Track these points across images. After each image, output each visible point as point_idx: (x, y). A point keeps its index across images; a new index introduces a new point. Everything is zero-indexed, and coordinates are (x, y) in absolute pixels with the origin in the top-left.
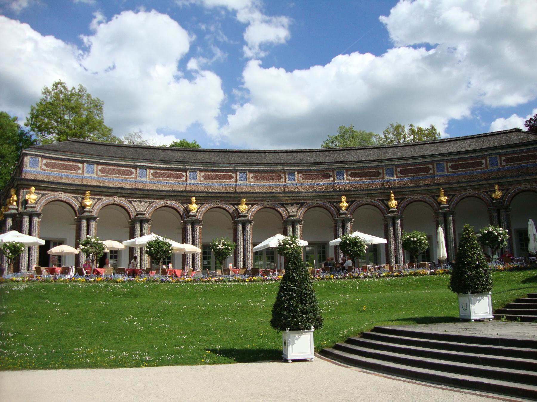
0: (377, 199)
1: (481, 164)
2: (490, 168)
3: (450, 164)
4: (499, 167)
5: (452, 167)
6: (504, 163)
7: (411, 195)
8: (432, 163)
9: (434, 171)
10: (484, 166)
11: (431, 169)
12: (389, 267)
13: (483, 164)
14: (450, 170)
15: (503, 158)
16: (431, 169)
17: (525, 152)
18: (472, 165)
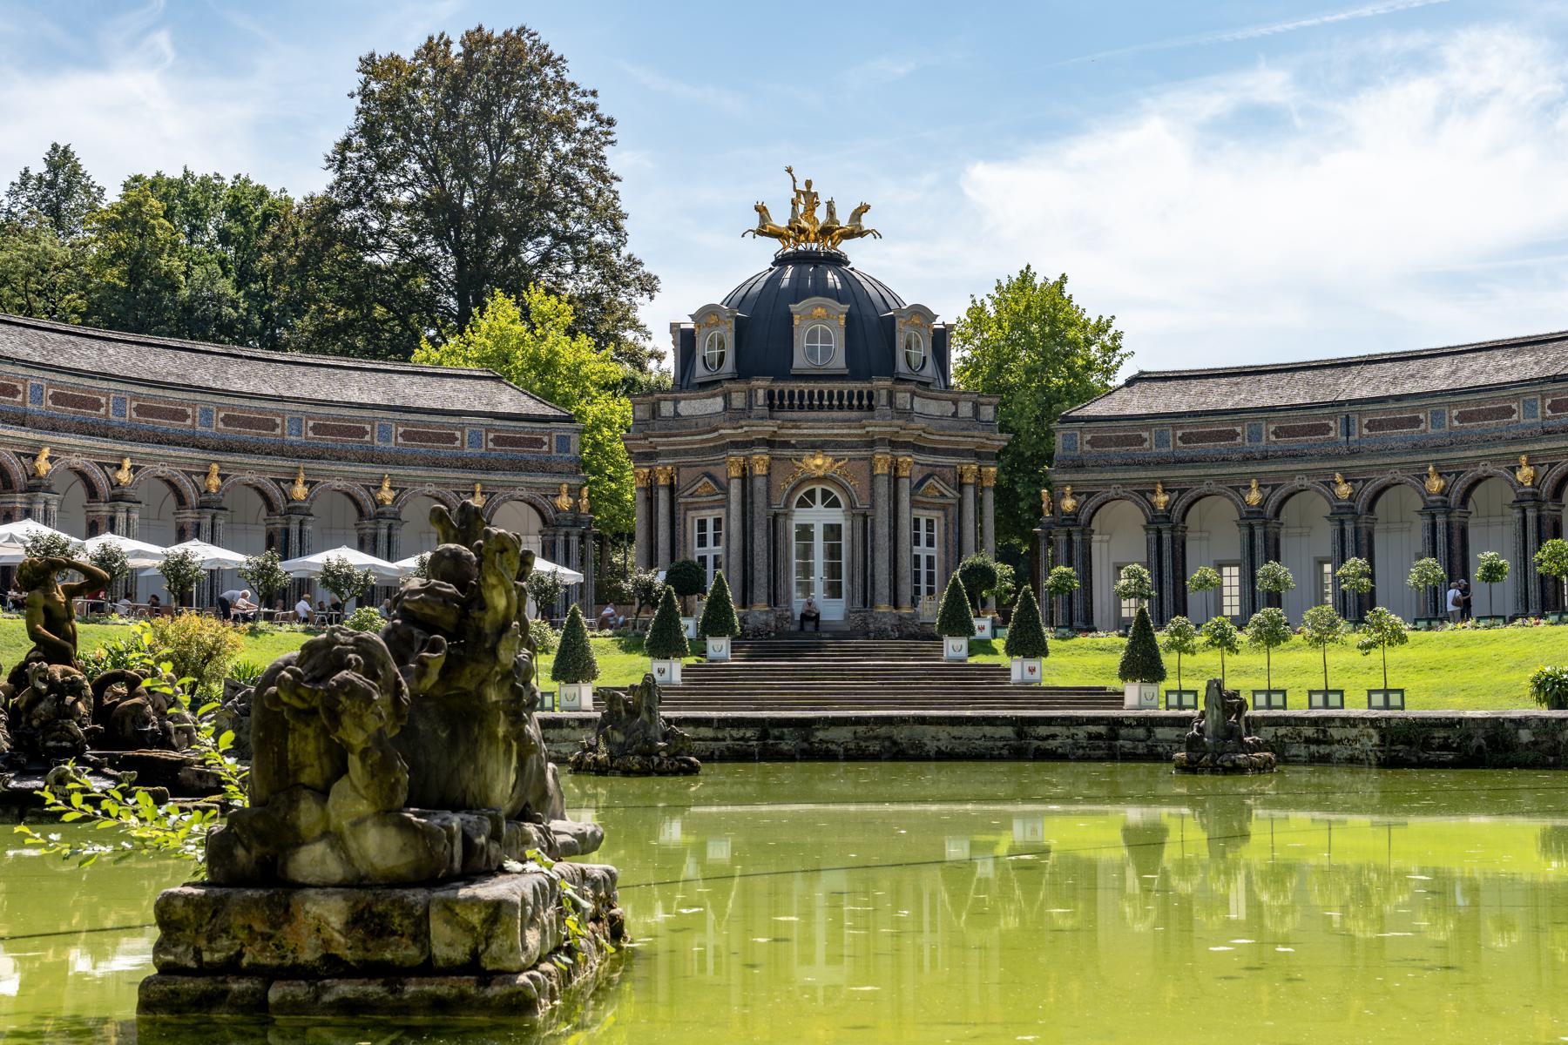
0: (268, 476)
1: (452, 439)
2: (468, 450)
3: (401, 430)
4: (483, 450)
5: (405, 435)
6: (491, 445)
7: (328, 477)
8: (372, 421)
9: (372, 437)
10: (458, 443)
11: (367, 433)
12: (265, 619)
13: (457, 439)
14: (400, 440)
15: (491, 436)
16: (367, 433)
17: (527, 433)
18: (439, 438)
